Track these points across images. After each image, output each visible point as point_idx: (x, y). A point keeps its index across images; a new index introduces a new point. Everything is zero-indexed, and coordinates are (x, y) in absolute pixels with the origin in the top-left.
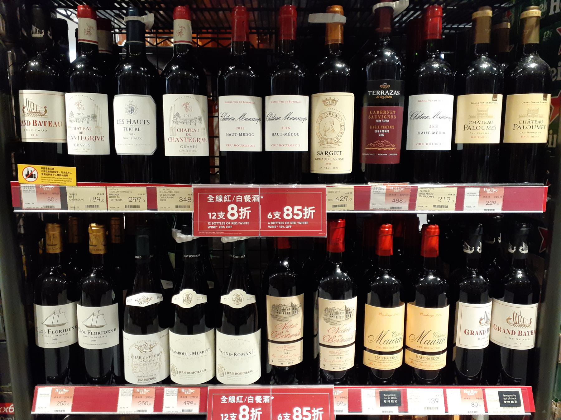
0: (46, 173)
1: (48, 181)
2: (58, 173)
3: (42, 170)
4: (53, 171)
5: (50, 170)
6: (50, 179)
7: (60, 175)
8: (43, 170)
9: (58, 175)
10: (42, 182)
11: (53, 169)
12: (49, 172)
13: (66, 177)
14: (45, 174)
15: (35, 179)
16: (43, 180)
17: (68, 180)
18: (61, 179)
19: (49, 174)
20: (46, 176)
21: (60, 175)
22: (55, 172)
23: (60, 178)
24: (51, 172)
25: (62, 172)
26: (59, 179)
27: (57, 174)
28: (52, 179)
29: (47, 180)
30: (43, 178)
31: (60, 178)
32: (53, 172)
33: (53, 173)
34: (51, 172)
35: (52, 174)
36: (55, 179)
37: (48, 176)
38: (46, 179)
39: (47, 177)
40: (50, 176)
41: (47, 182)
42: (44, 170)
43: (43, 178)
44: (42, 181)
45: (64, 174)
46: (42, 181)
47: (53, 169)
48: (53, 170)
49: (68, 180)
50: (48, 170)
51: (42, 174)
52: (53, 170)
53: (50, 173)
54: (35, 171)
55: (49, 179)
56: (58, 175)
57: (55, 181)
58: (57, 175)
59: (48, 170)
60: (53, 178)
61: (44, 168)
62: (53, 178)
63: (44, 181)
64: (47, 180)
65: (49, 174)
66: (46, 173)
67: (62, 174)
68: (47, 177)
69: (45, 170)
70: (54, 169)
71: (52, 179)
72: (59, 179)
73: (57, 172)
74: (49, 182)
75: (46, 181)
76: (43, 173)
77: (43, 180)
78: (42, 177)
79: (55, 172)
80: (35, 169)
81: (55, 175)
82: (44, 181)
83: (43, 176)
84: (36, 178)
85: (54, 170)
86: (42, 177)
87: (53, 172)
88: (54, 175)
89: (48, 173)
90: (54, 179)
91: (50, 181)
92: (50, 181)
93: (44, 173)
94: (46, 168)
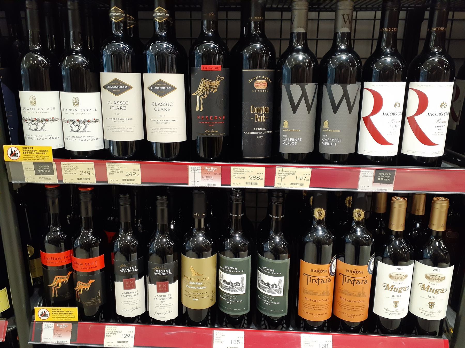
0: (55, 313)
1: (57, 318)
2: (64, 313)
6: (58, 317)
9: (64, 314)
12: (57, 311)
13: (70, 315)
14: (54, 313)
15: (47, 317)
16: (53, 317)
17: (72, 317)
18: (67, 317)
19: (58, 313)
20: (55, 315)
23: (66, 316)
25: (67, 311)
27: (63, 313)
28: (60, 317)
30: (53, 317)
31: (66, 316)
32: (61, 312)
37: (56, 315)
38: (55, 317)
40: (59, 315)
43: (53, 317)
44: (53, 318)
45: (68, 313)
46: (53, 318)
49: (72, 317)
50: (56, 310)
51: (53, 313)
55: (58, 317)
56: (64, 314)
58: (63, 313)
63: (54, 318)
65: (58, 313)
67: (67, 313)
71: (60, 317)
73: (64, 311)
76: (53, 312)
77: (53, 317)
82: (54, 318)
83: (54, 315)
84: (48, 316)
87: (61, 312)
89: (57, 313)
90: (61, 317)
93: (54, 312)
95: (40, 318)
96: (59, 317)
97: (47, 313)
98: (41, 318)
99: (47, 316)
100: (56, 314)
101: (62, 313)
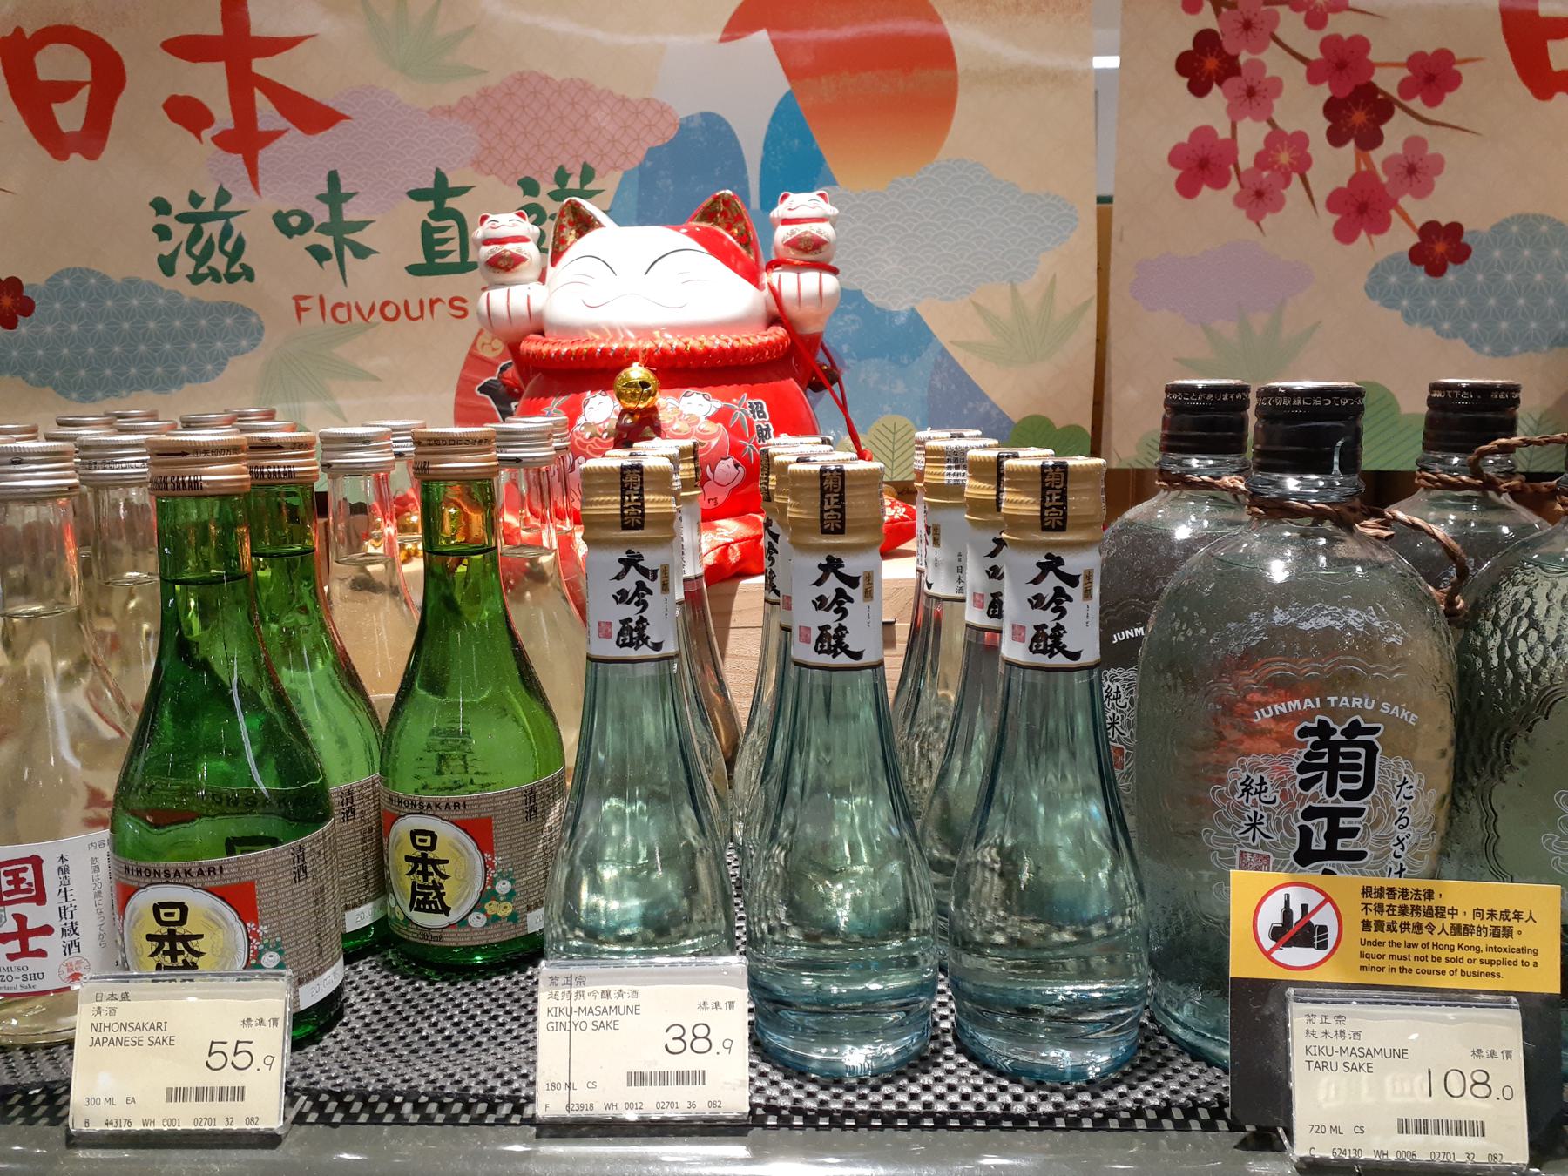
0: (1386, 918)
1: (1397, 964)
2: (1460, 920)
3: (1368, 900)
4: (1430, 908)
5: (1409, 903)
6: (1403, 951)
7: (1468, 930)
8: (1373, 901)
9: (1457, 930)
10: (1363, 968)
11: (1429, 894)
14: (1379, 926)
15: (1323, 954)
16: (1369, 956)
19: (1405, 926)
20: (1385, 936)
21: (1468, 930)
22: (1440, 912)
23: (1468, 948)
24: (1415, 909)
26: (1458, 953)
28: (1420, 952)
29: (1391, 956)
31: (1468, 948)
32: (1428, 912)
33: (1425, 921)
34: (1415, 909)
35: (1418, 926)
36: (1437, 953)
37: (1398, 937)
38: (1386, 950)
39: (1391, 943)
41: (1392, 970)
42: (1378, 901)
44: (1365, 962)
46: (1365, 962)
47: (1429, 894)
48: (1427, 903)
50: (1398, 902)
51: (1366, 925)
52: (1424, 903)
53: (1411, 920)
54: (1328, 905)
55: (1403, 951)
56: (1457, 930)
57: (1437, 966)
59: (1398, 902)
60: (1425, 946)
61: (1380, 892)
62: (1425, 946)
63: (1374, 962)
64: (1391, 956)
66: (1390, 919)
68: (1391, 943)
69: (1386, 901)
70: (1436, 895)
71: (1420, 952)
72: (1458, 953)
73: (1453, 912)
74: (1402, 969)
75: (1385, 963)
76: (1372, 917)
77: (1369, 956)
78: (1364, 943)
79: (1440, 912)
80: (1328, 899)
81: (1439, 929)
82: (1374, 962)
83: (1372, 936)
84: (1331, 940)
85: (1433, 903)
86: (1364, 943)
87: (1428, 912)
88: (1431, 928)
89: (1399, 919)
91: (1407, 964)
92: (1407, 964)
93: (1378, 917)
94: (1404, 892)
95: (1268, 954)
96: (1412, 952)
97: (1325, 917)
98: (1276, 955)
99: (1323, 946)
100: (1392, 927)
101: (1437, 922)
